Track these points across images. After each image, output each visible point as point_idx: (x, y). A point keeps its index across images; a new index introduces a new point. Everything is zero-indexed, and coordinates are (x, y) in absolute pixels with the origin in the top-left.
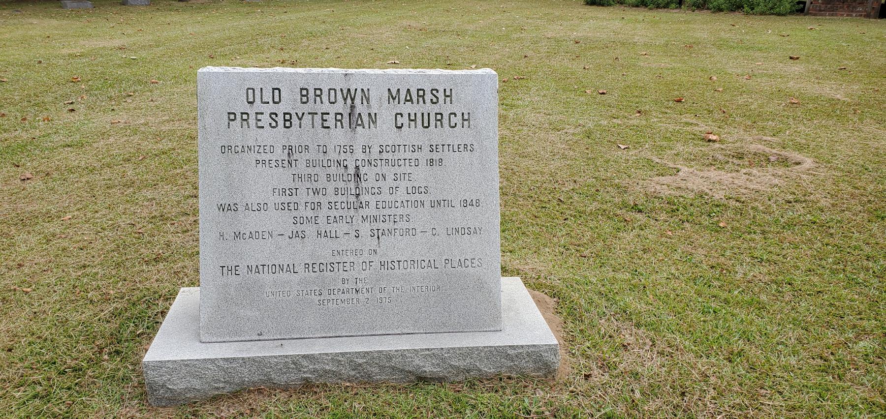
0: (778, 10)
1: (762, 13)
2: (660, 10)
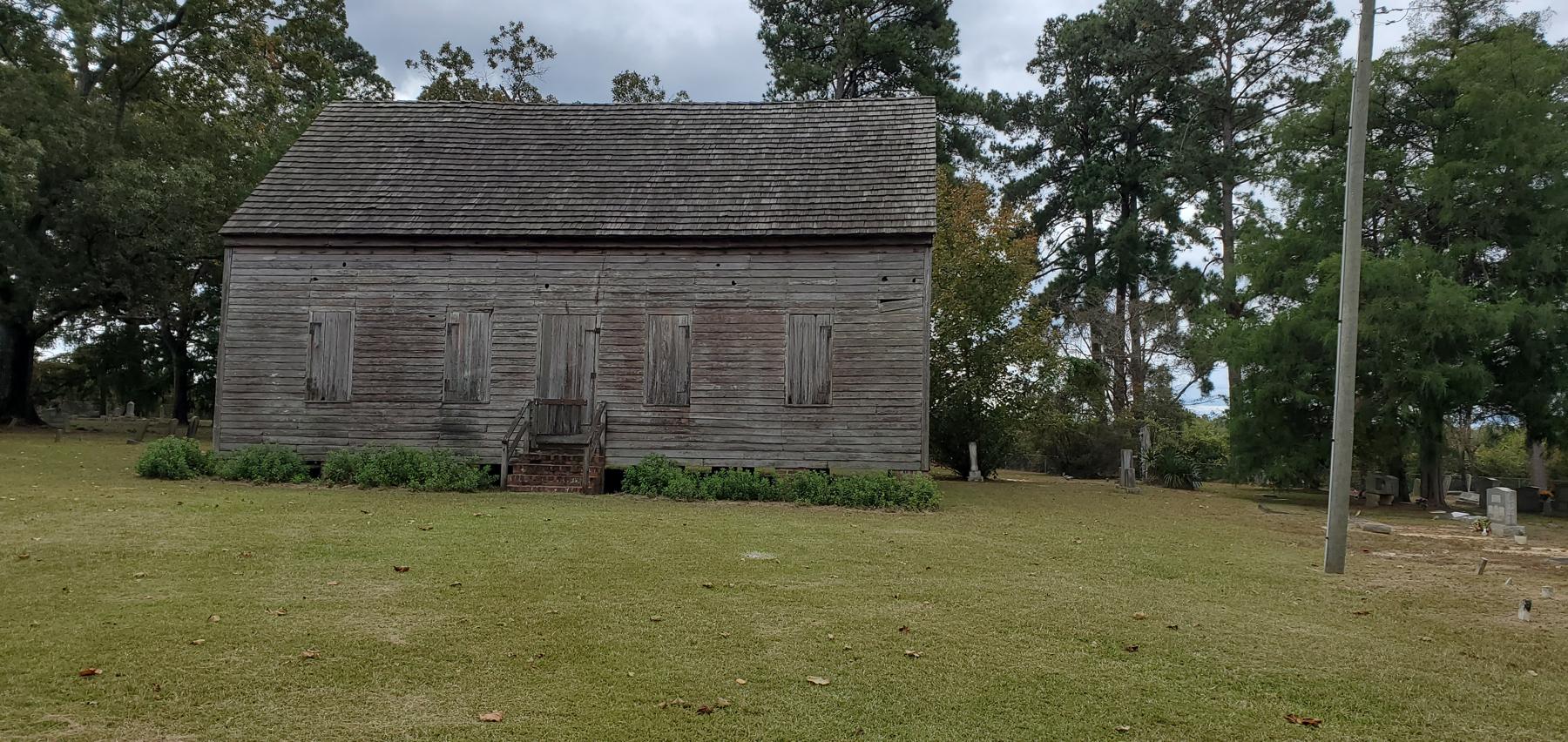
1: (438, 489)
2: (274, 485)
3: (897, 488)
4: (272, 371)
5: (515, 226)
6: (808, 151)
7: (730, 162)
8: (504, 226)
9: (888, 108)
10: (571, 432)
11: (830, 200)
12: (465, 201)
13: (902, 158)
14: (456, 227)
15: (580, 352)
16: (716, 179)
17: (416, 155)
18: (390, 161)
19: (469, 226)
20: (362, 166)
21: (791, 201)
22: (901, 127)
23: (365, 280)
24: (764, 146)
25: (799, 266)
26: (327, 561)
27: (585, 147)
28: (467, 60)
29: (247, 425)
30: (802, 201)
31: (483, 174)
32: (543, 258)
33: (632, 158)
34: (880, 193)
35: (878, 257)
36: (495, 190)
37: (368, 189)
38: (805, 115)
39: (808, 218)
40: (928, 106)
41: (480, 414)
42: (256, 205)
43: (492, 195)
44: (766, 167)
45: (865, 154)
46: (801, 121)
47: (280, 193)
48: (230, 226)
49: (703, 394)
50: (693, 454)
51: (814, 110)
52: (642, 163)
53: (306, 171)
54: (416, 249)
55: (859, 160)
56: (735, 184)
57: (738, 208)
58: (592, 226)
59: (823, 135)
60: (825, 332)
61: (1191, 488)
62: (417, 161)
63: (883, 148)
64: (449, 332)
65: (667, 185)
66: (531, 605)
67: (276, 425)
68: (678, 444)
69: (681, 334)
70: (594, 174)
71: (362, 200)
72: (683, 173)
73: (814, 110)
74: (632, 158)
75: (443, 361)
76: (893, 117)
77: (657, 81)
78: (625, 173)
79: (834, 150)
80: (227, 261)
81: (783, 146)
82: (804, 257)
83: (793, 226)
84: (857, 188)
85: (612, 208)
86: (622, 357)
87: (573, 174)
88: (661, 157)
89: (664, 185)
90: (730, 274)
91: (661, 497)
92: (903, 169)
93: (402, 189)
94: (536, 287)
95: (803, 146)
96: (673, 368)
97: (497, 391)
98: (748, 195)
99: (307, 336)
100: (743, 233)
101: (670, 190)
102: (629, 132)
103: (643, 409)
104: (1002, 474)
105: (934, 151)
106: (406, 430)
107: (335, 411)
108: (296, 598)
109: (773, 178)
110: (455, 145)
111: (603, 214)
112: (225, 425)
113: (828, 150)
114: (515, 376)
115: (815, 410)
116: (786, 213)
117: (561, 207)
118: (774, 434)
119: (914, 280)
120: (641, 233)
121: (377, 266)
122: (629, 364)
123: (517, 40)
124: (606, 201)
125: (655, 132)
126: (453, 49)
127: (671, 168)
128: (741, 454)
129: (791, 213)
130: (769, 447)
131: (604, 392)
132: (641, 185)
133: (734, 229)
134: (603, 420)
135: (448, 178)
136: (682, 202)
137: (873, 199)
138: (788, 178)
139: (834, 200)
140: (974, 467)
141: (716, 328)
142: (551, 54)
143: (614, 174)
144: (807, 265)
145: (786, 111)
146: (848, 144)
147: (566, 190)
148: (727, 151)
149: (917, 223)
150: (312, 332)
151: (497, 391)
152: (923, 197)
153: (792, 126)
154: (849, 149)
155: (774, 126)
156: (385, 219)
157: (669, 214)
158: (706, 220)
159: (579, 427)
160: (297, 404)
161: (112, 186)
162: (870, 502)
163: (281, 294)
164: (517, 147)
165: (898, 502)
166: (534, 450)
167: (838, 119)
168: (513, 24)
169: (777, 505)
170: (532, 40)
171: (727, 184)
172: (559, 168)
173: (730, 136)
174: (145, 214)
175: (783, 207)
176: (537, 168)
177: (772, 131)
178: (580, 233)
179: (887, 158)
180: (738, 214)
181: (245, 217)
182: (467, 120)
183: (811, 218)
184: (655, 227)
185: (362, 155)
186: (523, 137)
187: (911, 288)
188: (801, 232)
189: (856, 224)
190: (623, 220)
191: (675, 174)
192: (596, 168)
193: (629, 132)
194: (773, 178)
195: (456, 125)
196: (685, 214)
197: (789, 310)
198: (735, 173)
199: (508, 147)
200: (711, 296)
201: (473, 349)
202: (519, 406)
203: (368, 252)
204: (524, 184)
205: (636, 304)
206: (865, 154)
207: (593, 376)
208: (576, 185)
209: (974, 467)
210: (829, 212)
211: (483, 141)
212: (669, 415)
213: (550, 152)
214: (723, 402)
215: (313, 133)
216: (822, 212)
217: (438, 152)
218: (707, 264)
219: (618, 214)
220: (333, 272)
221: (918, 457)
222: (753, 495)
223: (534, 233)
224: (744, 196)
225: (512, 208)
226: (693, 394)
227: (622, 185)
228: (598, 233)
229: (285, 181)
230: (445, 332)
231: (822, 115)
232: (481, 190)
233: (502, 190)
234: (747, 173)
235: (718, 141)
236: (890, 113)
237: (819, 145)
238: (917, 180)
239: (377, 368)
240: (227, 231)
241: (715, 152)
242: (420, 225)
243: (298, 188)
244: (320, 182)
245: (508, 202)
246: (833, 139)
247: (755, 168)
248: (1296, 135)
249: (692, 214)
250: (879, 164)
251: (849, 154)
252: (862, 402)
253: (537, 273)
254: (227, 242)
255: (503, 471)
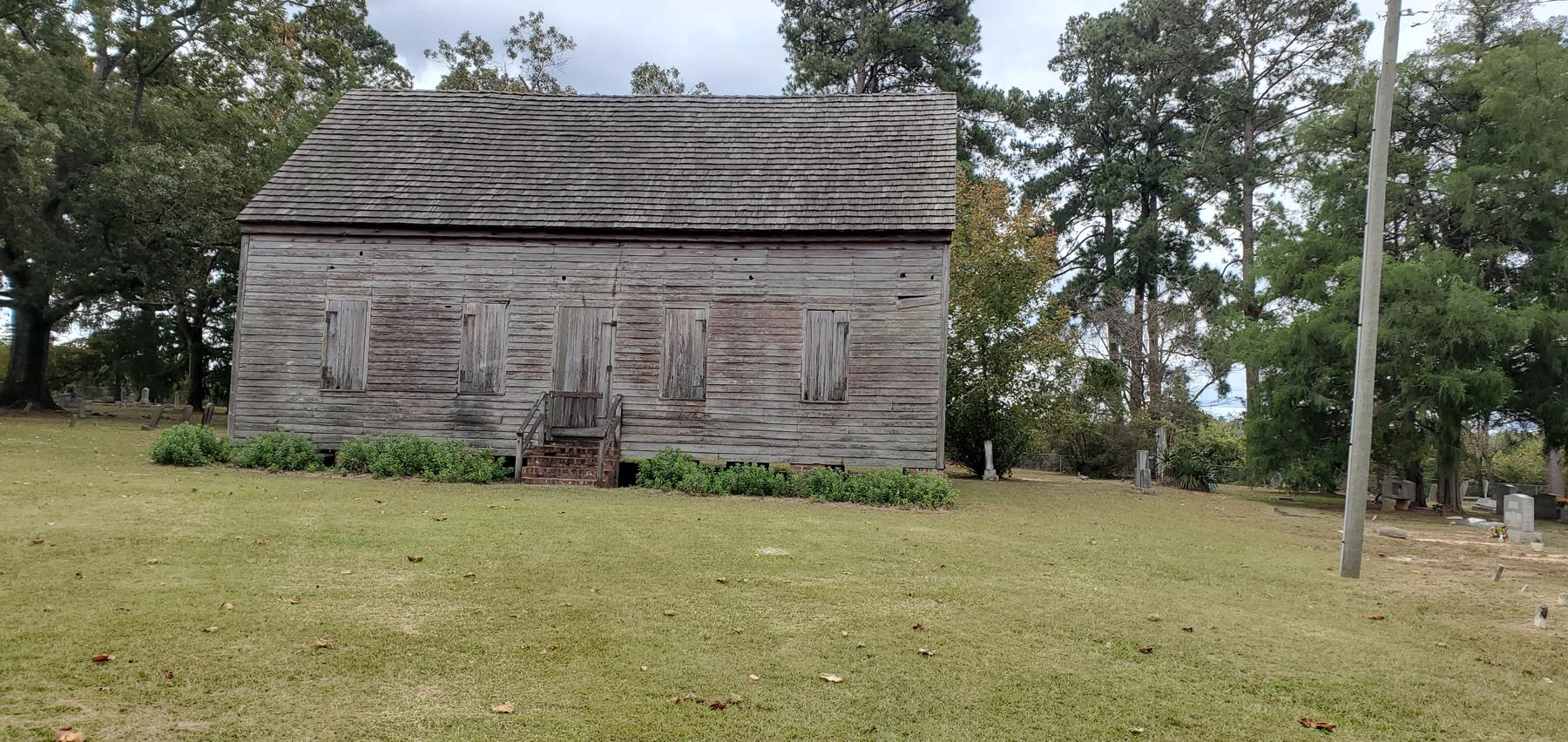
0: (473, 474)
1: (453, 480)
2: (288, 473)
3: (912, 486)
4: (286, 358)
5: (533, 218)
6: (828, 145)
7: (749, 156)
8: (522, 217)
9: (908, 104)
10: (586, 425)
11: (849, 195)
12: (483, 192)
13: (922, 154)
14: (475, 217)
15: (596, 344)
16: (734, 173)
17: (435, 145)
18: (408, 150)
19: (486, 216)
20: (380, 155)
21: (810, 196)
22: (922, 123)
23: (382, 269)
24: (784, 140)
25: (817, 261)
26: (341, 550)
27: (603, 139)
28: (486, 50)
29: (261, 412)
30: (820, 196)
31: (502, 164)
32: (562, 250)
33: (651, 150)
34: (899, 189)
35: (897, 253)
36: (513, 181)
37: (386, 177)
38: (825, 110)
39: (826, 214)
40: (949, 102)
41: (495, 405)
42: (274, 193)
43: (510, 186)
44: (785, 161)
45: (885, 149)
46: (821, 115)
47: (297, 181)
48: (247, 213)
49: (719, 389)
50: (708, 448)
51: (835, 105)
52: (661, 155)
53: (324, 159)
54: (433, 239)
55: (879, 155)
56: (754, 178)
57: (757, 202)
58: (610, 218)
59: (843, 130)
60: (842, 328)
61: (1208, 490)
62: (435, 150)
63: (903, 143)
64: (466, 323)
65: (686, 178)
66: (544, 598)
67: (291, 412)
68: (692, 438)
69: (698, 327)
70: (612, 166)
71: (380, 189)
72: (702, 167)
73: (835, 105)
74: (651, 150)
75: (459, 352)
76: (914, 113)
77: (676, 73)
78: (644, 166)
79: (854, 145)
80: (244, 248)
81: (802, 140)
82: (823, 253)
83: (812, 221)
84: (876, 183)
85: (630, 200)
86: (638, 350)
87: (591, 165)
88: (680, 150)
89: (682, 178)
90: (748, 269)
91: (676, 491)
92: (923, 165)
93: (420, 178)
94: (552, 279)
95: (822, 140)
96: (689, 362)
97: (512, 383)
98: (767, 190)
99: (324, 324)
100: (761, 228)
101: (689, 183)
102: (648, 124)
103: (659, 403)
104: (1016, 473)
105: (954, 147)
106: (420, 420)
107: (350, 400)
108: (310, 587)
109: (792, 173)
110: (473, 135)
111: (621, 206)
112: (240, 412)
113: (848, 145)
114: (532, 368)
115: (831, 407)
116: (805, 208)
117: (579, 199)
118: (790, 429)
119: (932, 278)
120: (659, 226)
121: (394, 255)
122: (646, 357)
123: (537, 30)
124: (625, 194)
125: (674, 124)
126: (472, 38)
127: (690, 161)
128: (756, 449)
129: (810, 208)
130: (785, 443)
131: (620, 386)
132: (659, 178)
133: (752, 223)
134: (618, 413)
135: (466, 168)
136: (700, 195)
137: (893, 195)
138: (807, 173)
139: (853, 195)
140: (989, 465)
141: (733, 322)
142: (571, 45)
143: (633, 166)
144: (824, 259)
145: (806, 105)
146: (869, 139)
147: (584, 182)
148: (747, 145)
149: (936, 220)
150: (328, 321)
151: (512, 383)
152: (942, 194)
153: (812, 120)
154: (869, 145)
155: (794, 120)
156: (402, 208)
157: (687, 208)
158: (724, 214)
159: (594, 420)
160: (313, 392)
161: (129, 171)
162: (885, 500)
163: (298, 282)
164: (536, 138)
165: (913, 500)
166: (549, 442)
167: (858, 114)
168: (532, 14)
169: (792, 501)
170: (552, 30)
171: (745, 178)
172: (577, 160)
173: (750, 130)
174: (161, 199)
175: (802, 202)
176: (556, 159)
177: (792, 125)
178: (598, 225)
179: (908, 154)
180: (757, 208)
181: (263, 205)
182: (486, 110)
183: (829, 214)
184: (672, 220)
185: (380, 143)
186: (542, 128)
187: (930, 284)
188: (819, 227)
189: (876, 220)
190: (641, 212)
191: (693, 167)
192: (614, 160)
193: (648, 124)
194: (792, 173)
195: (475, 115)
196: (704, 208)
197: (806, 306)
198: (753, 167)
199: (526, 138)
200: (728, 291)
201: (490, 342)
202: (535, 398)
203: (385, 241)
204: (542, 176)
205: (653, 297)
206: (885, 149)
207: (609, 369)
208: (594, 177)
209: (989, 465)
210: (848, 207)
211: (502, 132)
212: (685, 409)
213: (568, 144)
214: (739, 396)
215: (332, 121)
216: (841, 207)
217: (456, 142)
218: (725, 257)
219: (636, 206)
220: (350, 261)
221: (934, 455)
222: (768, 491)
223: (551, 224)
224: (762, 190)
225: (530, 199)
226: (709, 389)
227: (640, 177)
228: (616, 225)
229: (303, 169)
230: (461, 323)
231: (842, 110)
232: (499, 181)
233: (519, 181)
234: (766, 166)
235: (737, 135)
236: (911, 108)
237: (839, 140)
238: (937, 176)
239: (393, 358)
240: (244, 218)
241: (734, 145)
242: (437, 215)
243: (316, 176)
244: (338, 171)
245: (526, 193)
246: (852, 134)
247: (774, 162)
248: (1320, 138)
249: (710, 208)
250: (899, 160)
251: (869, 150)
252: (878, 399)
253: (554, 265)
254: (244, 229)
255: (518, 463)
